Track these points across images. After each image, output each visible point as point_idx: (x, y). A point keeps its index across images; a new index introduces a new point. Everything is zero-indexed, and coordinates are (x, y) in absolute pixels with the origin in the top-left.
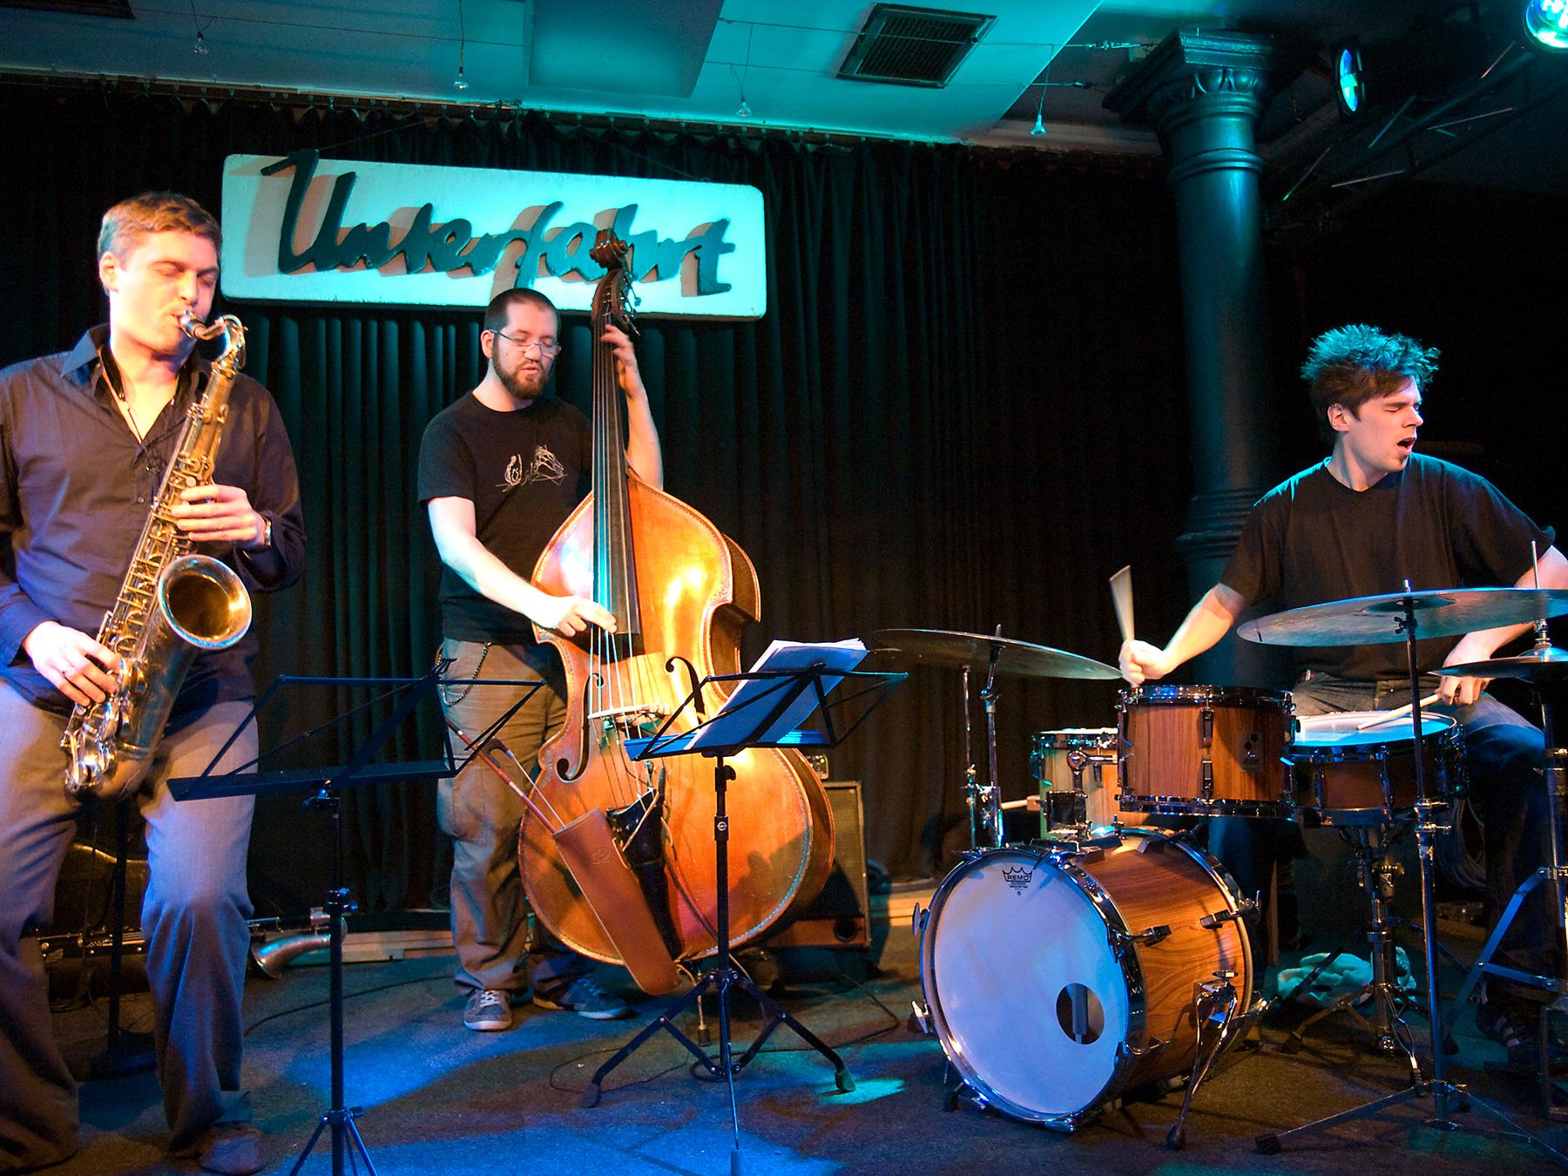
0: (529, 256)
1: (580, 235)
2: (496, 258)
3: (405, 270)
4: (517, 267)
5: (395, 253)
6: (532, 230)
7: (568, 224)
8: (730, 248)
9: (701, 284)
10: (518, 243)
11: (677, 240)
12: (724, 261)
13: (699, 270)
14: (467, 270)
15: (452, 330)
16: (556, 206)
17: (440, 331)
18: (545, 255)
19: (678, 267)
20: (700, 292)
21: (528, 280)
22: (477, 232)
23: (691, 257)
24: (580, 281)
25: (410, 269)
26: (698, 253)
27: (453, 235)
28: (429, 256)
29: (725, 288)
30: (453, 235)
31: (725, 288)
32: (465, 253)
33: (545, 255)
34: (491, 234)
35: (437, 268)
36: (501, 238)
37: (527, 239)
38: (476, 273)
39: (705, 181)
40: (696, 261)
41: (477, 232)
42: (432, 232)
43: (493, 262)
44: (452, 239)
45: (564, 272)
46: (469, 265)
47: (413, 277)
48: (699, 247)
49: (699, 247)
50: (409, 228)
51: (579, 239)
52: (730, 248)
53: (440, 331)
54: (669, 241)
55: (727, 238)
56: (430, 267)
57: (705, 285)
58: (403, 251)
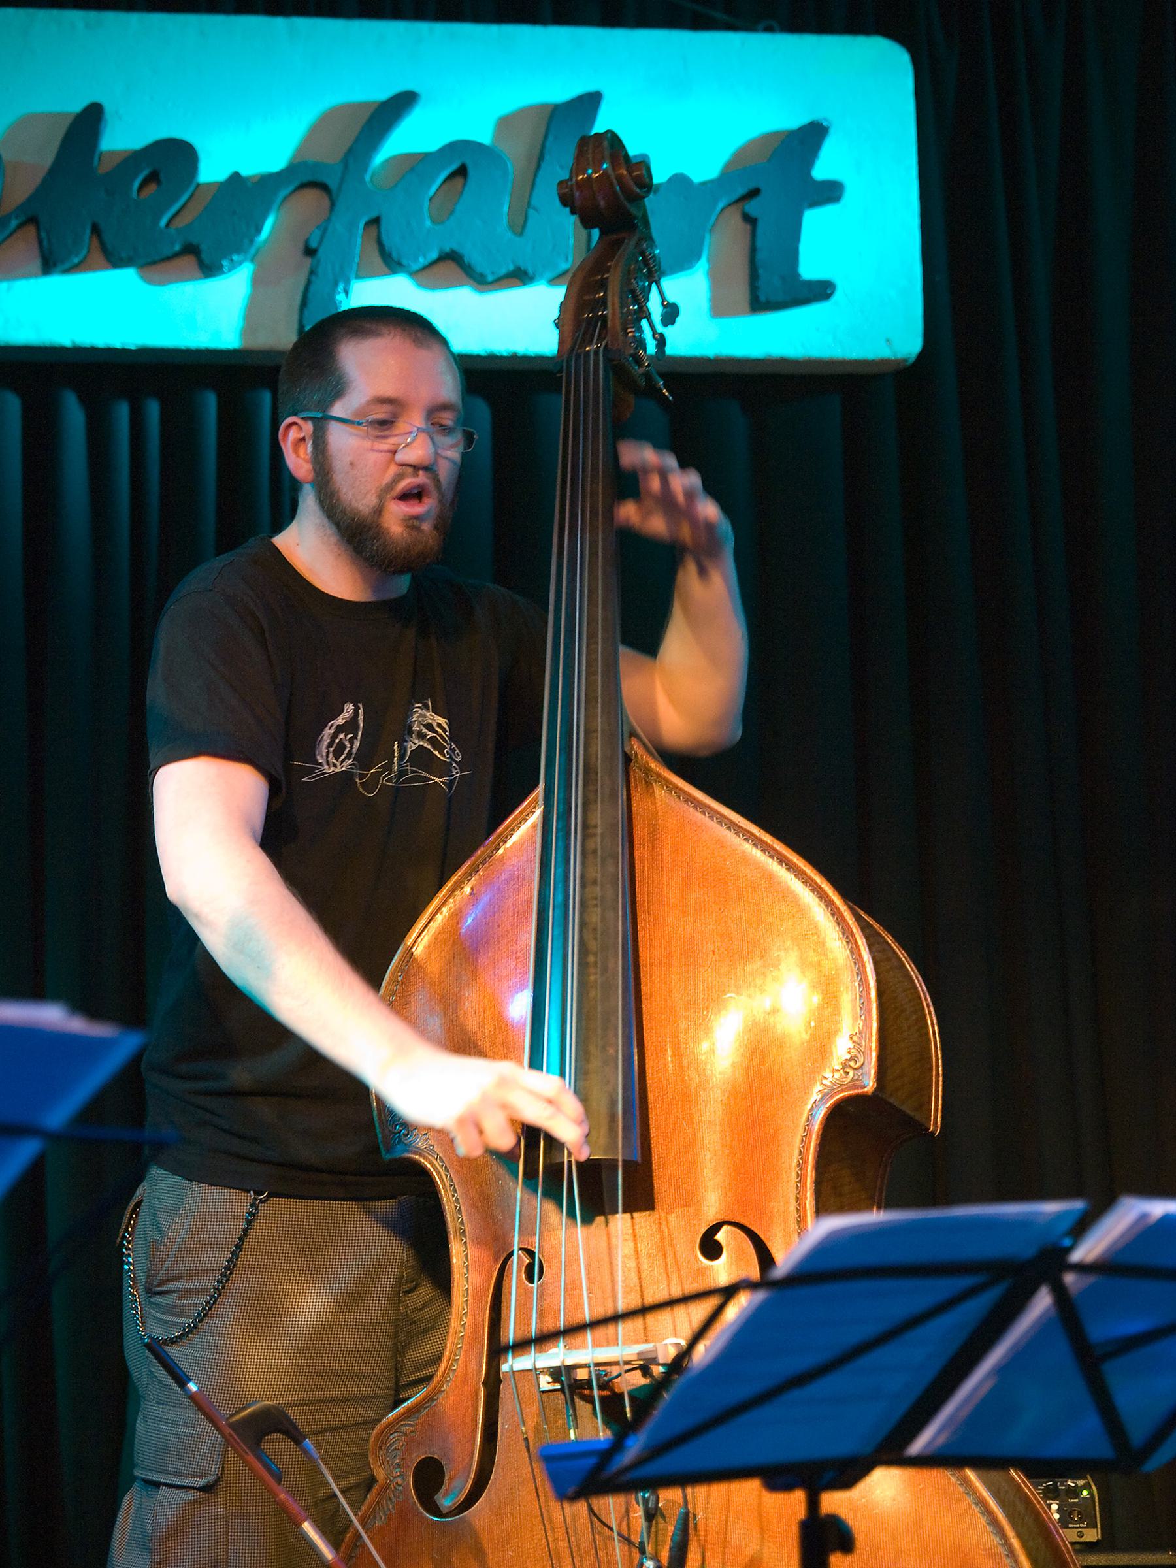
0: (338, 225)
1: (462, 172)
2: (259, 230)
3: (37, 264)
4: (310, 252)
5: (14, 223)
6: (345, 162)
7: (431, 144)
8: (831, 192)
9: (760, 283)
10: (311, 195)
11: (697, 177)
12: (814, 221)
13: (753, 250)
14: (189, 261)
15: (153, 409)
16: (403, 102)
17: (123, 411)
18: (375, 222)
19: (703, 238)
20: (759, 304)
21: (336, 285)
22: (211, 171)
23: (735, 220)
24: (460, 284)
25: (49, 264)
26: (752, 207)
27: (153, 177)
28: (96, 230)
29: (821, 291)
30: (153, 177)
31: (821, 291)
32: (180, 223)
33: (375, 222)
34: (245, 172)
35: (114, 261)
36: (267, 184)
37: (332, 183)
38: (209, 269)
39: (769, 29)
40: (749, 227)
41: (211, 171)
42: (102, 170)
43: (252, 241)
44: (153, 187)
45: (422, 261)
46: (191, 250)
47: (57, 283)
48: (754, 193)
49: (754, 193)
50: (48, 159)
51: (459, 181)
52: (831, 192)
53: (123, 411)
54: (680, 181)
55: (822, 170)
56: (97, 255)
57: (770, 285)
58: (33, 220)
